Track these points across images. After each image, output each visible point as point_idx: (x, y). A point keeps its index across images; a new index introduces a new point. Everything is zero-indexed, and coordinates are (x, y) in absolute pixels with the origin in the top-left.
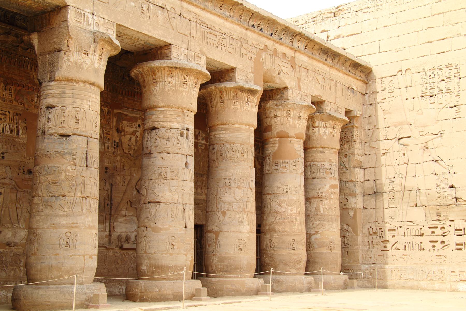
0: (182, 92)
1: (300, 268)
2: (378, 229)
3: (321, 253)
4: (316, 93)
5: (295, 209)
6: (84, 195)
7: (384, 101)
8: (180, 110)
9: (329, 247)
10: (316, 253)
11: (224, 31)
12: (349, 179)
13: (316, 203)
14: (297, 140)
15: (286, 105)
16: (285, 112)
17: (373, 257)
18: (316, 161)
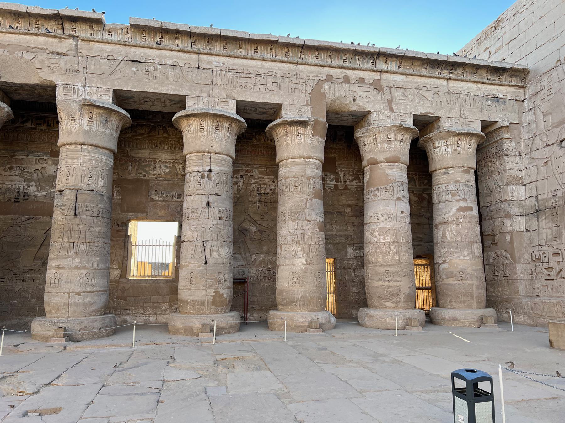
0: (200, 137)
1: (399, 302)
2: (541, 254)
3: (449, 284)
4: (421, 111)
5: (388, 237)
6: (71, 240)
7: (544, 101)
8: (200, 154)
9: (459, 278)
10: (444, 284)
11: (261, 71)
12: (503, 199)
13: (442, 229)
14: (390, 164)
15: (371, 130)
16: (371, 138)
17: (536, 289)
18: (441, 184)
